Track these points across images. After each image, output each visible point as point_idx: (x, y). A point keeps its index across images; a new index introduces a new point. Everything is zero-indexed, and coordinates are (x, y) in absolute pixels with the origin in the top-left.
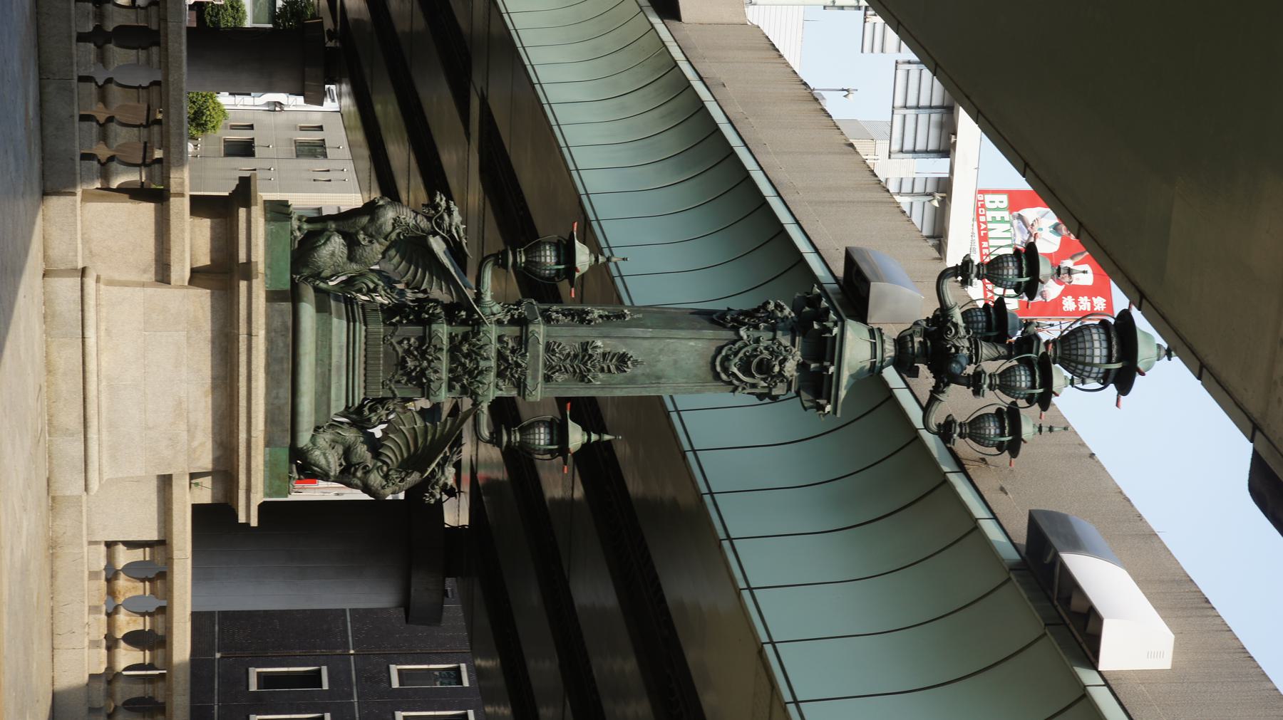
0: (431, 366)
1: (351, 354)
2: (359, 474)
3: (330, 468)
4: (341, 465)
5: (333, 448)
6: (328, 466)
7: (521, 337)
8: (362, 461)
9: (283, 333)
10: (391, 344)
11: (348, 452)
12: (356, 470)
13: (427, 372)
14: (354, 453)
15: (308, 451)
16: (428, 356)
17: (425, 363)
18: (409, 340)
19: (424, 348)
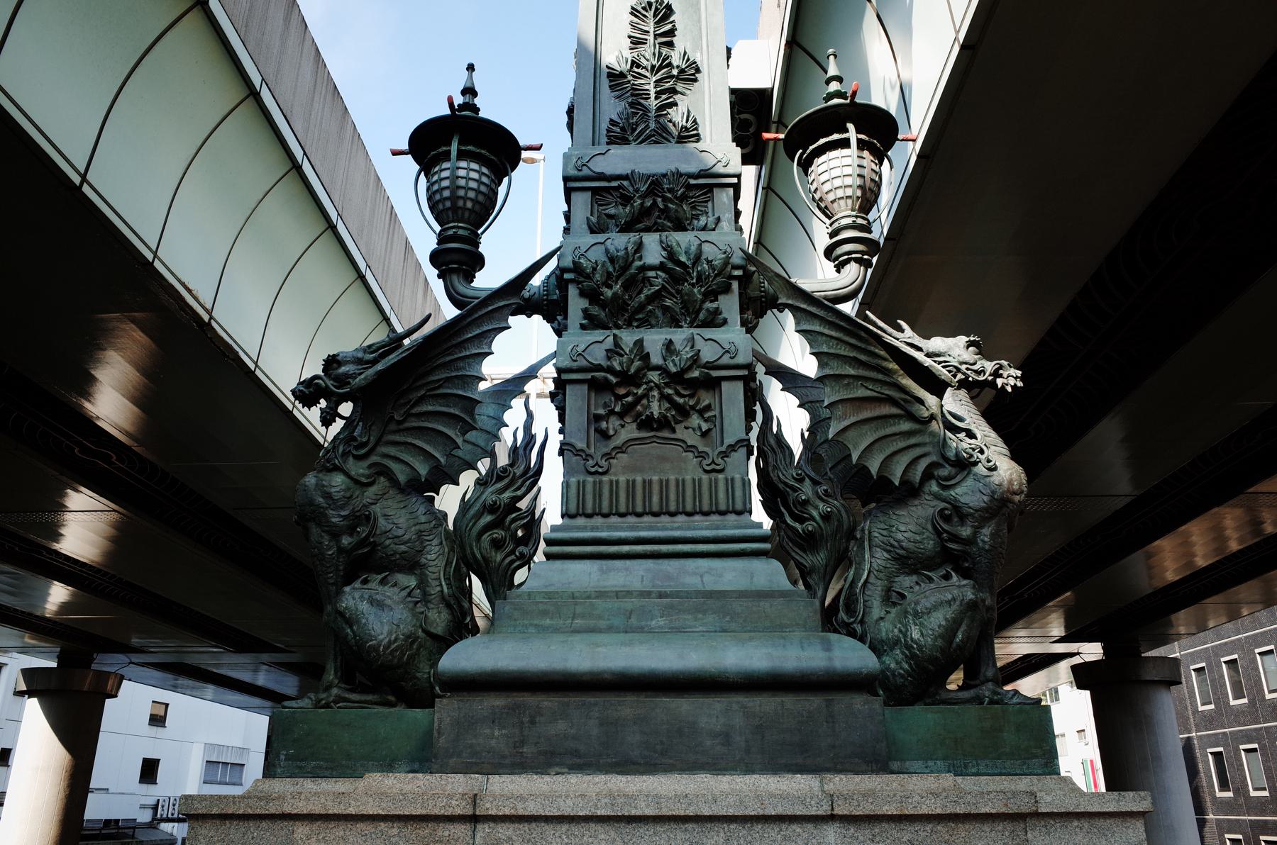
0: (661, 362)
1: (625, 549)
2: (966, 532)
3: (954, 599)
4: (947, 577)
5: (903, 596)
6: (949, 603)
7: (595, 191)
8: (929, 527)
9: (526, 719)
10: (608, 456)
11: (909, 562)
12: (955, 538)
13: (673, 370)
14: (911, 546)
15: (913, 656)
16: (632, 370)
17: (654, 376)
18: (598, 418)
19: (613, 379)
